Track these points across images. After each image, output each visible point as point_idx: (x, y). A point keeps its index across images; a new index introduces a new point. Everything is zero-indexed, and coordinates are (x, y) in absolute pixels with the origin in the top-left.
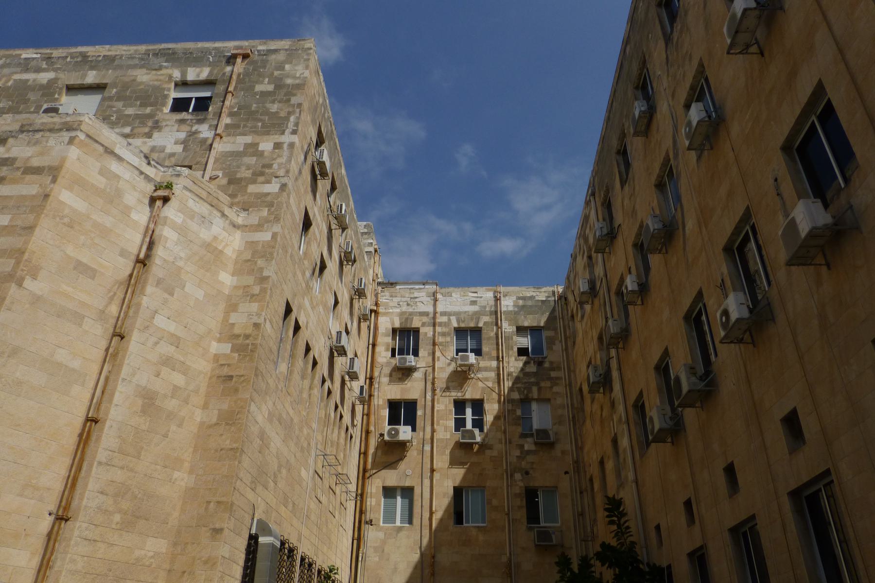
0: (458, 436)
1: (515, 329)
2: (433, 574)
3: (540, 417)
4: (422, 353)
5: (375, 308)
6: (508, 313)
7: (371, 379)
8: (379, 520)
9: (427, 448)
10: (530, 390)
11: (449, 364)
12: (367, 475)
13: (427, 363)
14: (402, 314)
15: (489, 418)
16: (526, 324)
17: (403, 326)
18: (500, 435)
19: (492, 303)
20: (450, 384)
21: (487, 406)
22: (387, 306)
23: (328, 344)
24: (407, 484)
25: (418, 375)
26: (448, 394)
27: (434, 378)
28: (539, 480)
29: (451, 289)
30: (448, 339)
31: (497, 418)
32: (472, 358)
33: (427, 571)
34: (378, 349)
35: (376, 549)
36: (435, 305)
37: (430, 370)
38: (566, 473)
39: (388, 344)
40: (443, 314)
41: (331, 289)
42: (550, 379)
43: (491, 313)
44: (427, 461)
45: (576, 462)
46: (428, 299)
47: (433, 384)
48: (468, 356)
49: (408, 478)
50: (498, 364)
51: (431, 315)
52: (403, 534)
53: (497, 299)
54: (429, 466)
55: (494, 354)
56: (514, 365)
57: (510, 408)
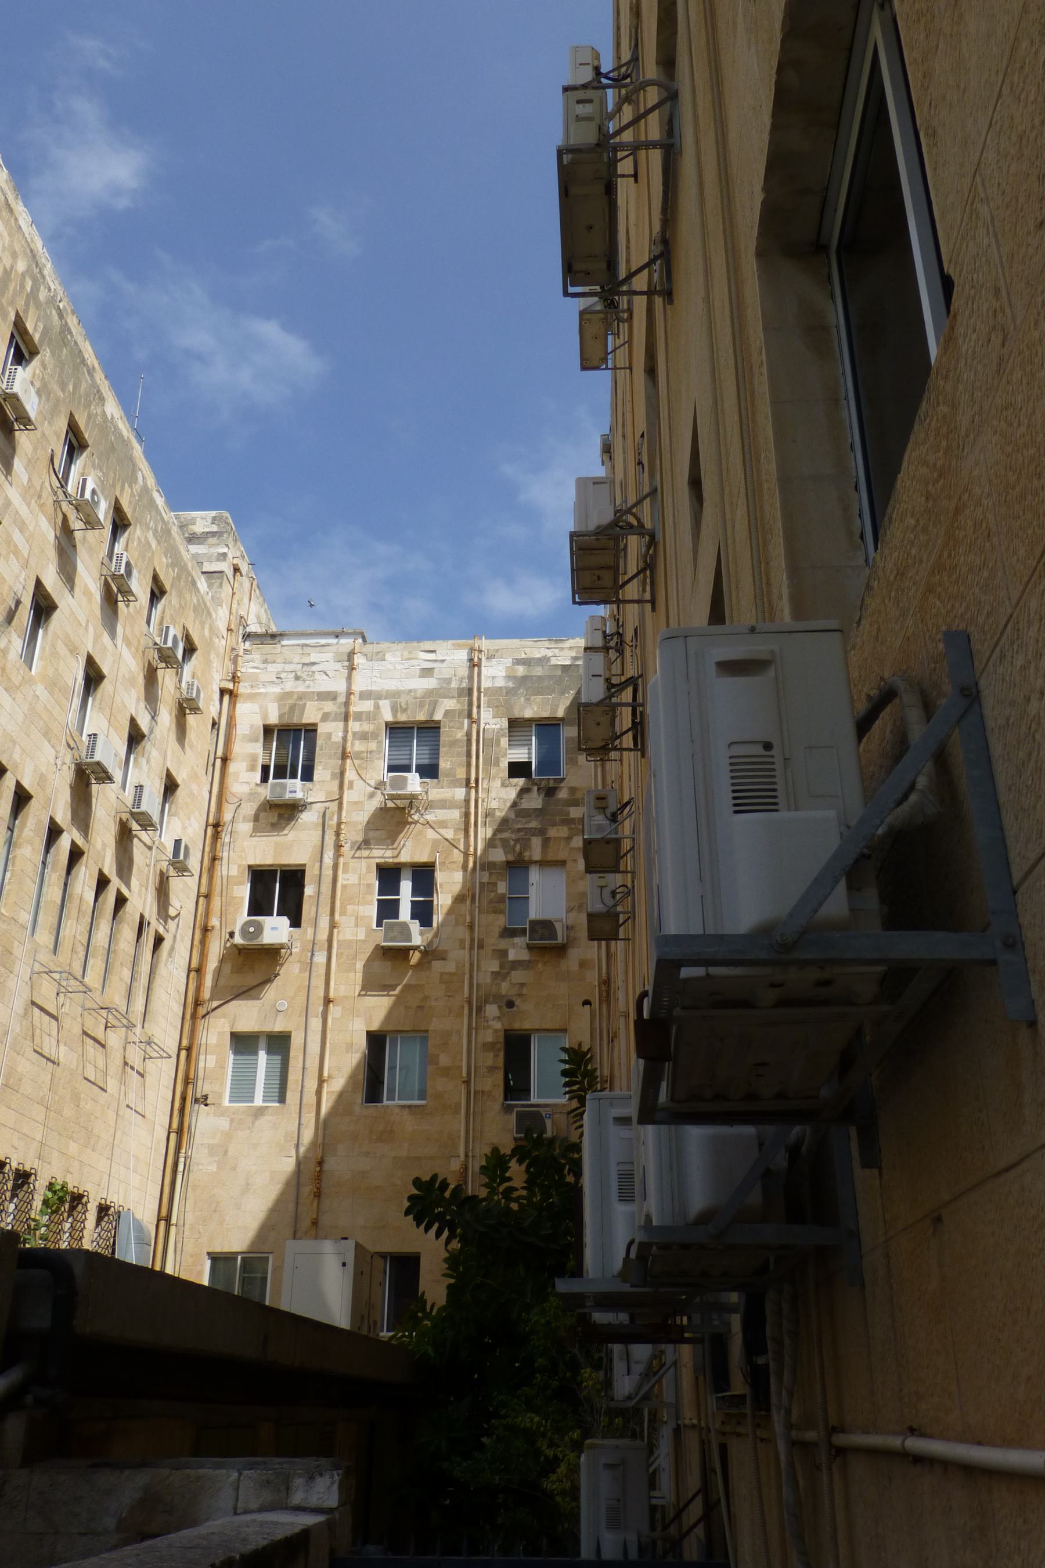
0: (379, 938)
1: (506, 724)
2: (318, 1194)
3: (548, 897)
4: (319, 773)
5: (230, 686)
6: (493, 691)
7: (216, 826)
8: (220, 1095)
9: (320, 958)
10: (526, 845)
11: (372, 796)
12: (202, 1011)
13: (328, 793)
14: (285, 696)
15: (442, 901)
16: (528, 714)
17: (286, 721)
18: (463, 933)
19: (464, 672)
20: (371, 834)
21: (440, 876)
22: (254, 681)
23: (68, 759)
24: (278, 1027)
25: (308, 817)
26: (365, 853)
27: (339, 824)
28: (529, 1018)
29: (384, 645)
30: (373, 745)
31: (459, 899)
32: (414, 782)
33: (307, 1189)
34: (233, 767)
35: (212, 1150)
36: (349, 678)
37: (334, 806)
38: (586, 1003)
39: (254, 758)
40: (365, 695)
41: (74, 651)
42: (568, 821)
43: (460, 692)
44: (319, 982)
45: (606, 983)
46: (338, 666)
47: (338, 834)
48: (405, 779)
49: (281, 1016)
50: (468, 794)
51: (342, 699)
52: (265, 1121)
53: (474, 665)
54: (322, 994)
55: (461, 773)
56: (500, 794)
57: (485, 880)
